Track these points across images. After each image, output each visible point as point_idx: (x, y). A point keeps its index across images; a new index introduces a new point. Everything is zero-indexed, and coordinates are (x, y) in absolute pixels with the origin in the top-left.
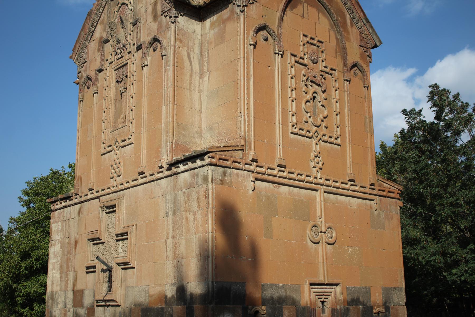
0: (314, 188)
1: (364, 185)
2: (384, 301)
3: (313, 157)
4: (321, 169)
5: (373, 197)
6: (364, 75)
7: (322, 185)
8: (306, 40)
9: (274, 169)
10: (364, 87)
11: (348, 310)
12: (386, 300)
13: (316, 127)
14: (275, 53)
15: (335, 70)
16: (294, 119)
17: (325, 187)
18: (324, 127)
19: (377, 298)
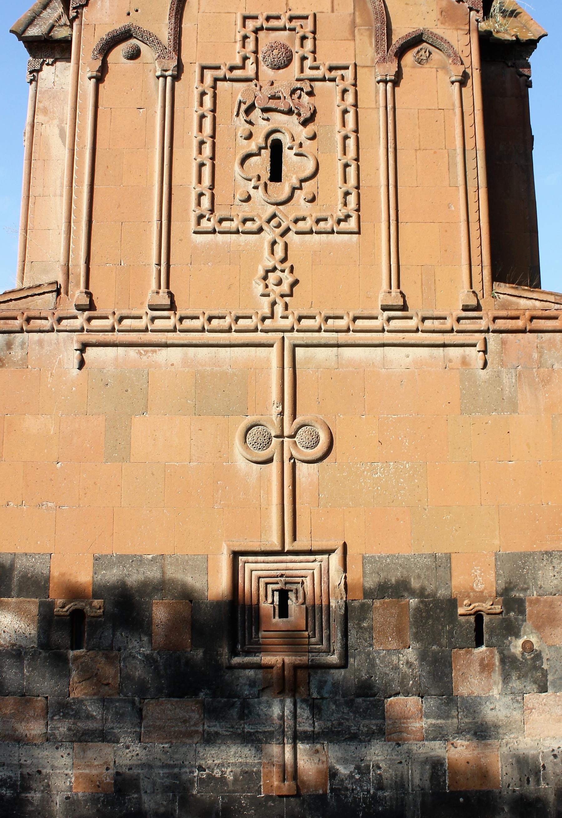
0: (257, 341)
1: (436, 313)
2: (503, 586)
3: (261, 273)
4: (282, 296)
5: (479, 337)
6: (449, 56)
7: (292, 330)
8: (251, 25)
9: (141, 318)
10: (453, 83)
11: (364, 609)
12: (510, 583)
13: (274, 207)
14: (158, 77)
15: (347, 68)
16: (206, 202)
17: (301, 334)
18: (302, 202)
19: (475, 582)
